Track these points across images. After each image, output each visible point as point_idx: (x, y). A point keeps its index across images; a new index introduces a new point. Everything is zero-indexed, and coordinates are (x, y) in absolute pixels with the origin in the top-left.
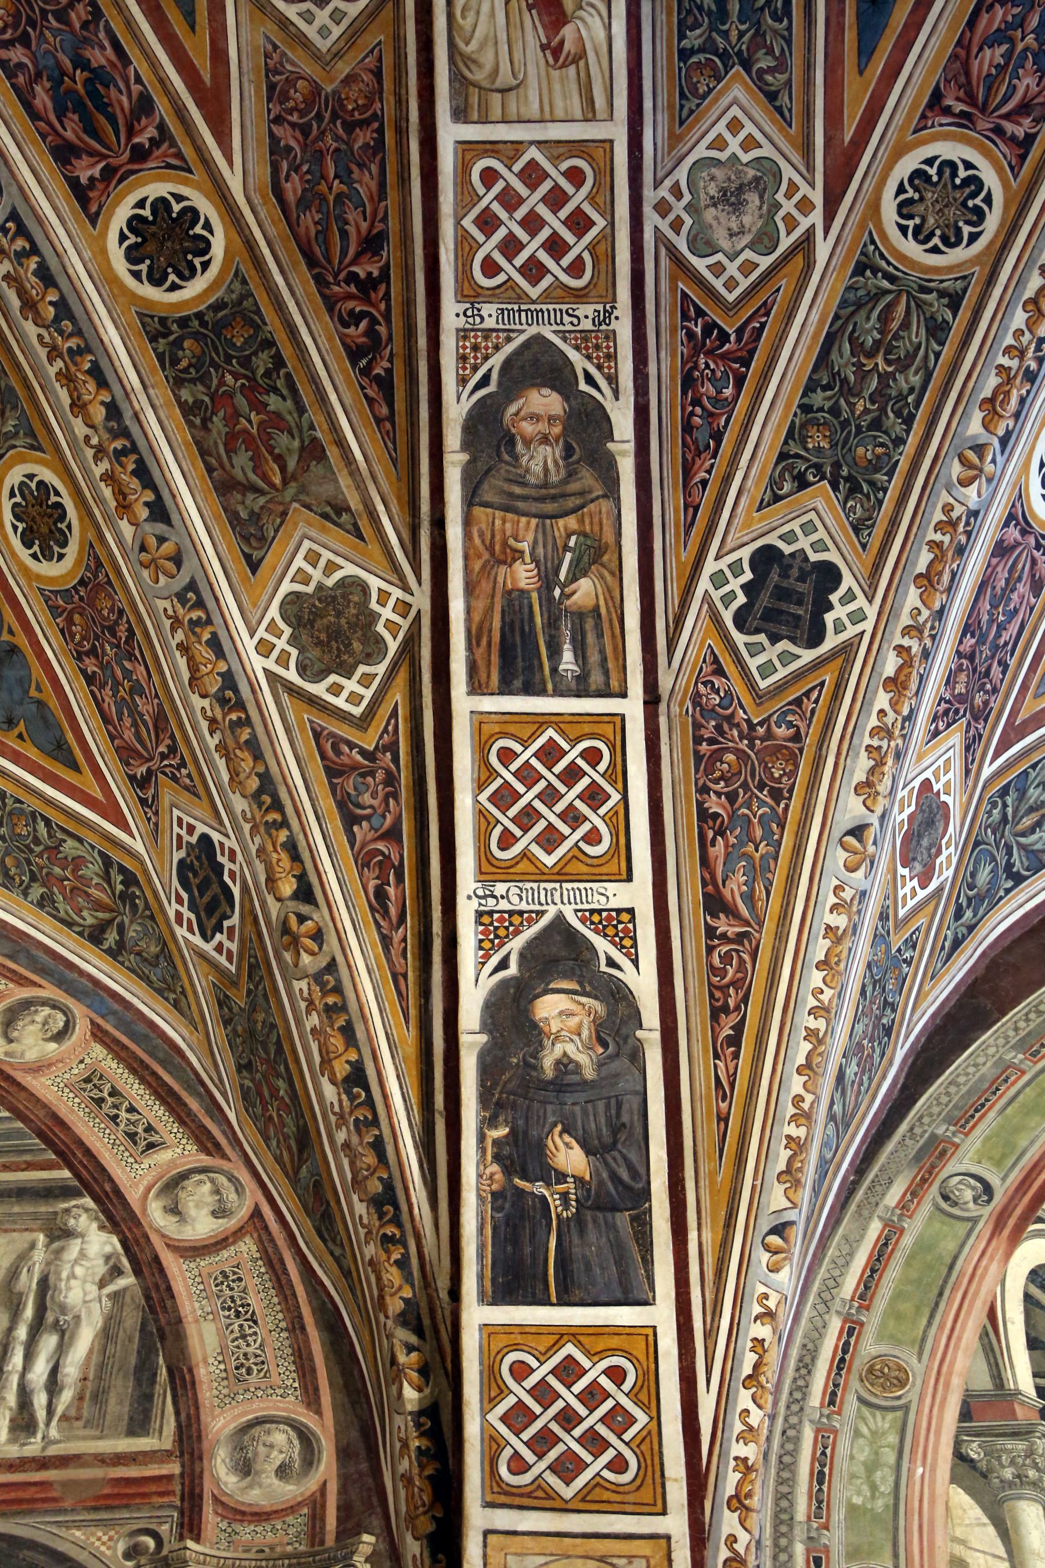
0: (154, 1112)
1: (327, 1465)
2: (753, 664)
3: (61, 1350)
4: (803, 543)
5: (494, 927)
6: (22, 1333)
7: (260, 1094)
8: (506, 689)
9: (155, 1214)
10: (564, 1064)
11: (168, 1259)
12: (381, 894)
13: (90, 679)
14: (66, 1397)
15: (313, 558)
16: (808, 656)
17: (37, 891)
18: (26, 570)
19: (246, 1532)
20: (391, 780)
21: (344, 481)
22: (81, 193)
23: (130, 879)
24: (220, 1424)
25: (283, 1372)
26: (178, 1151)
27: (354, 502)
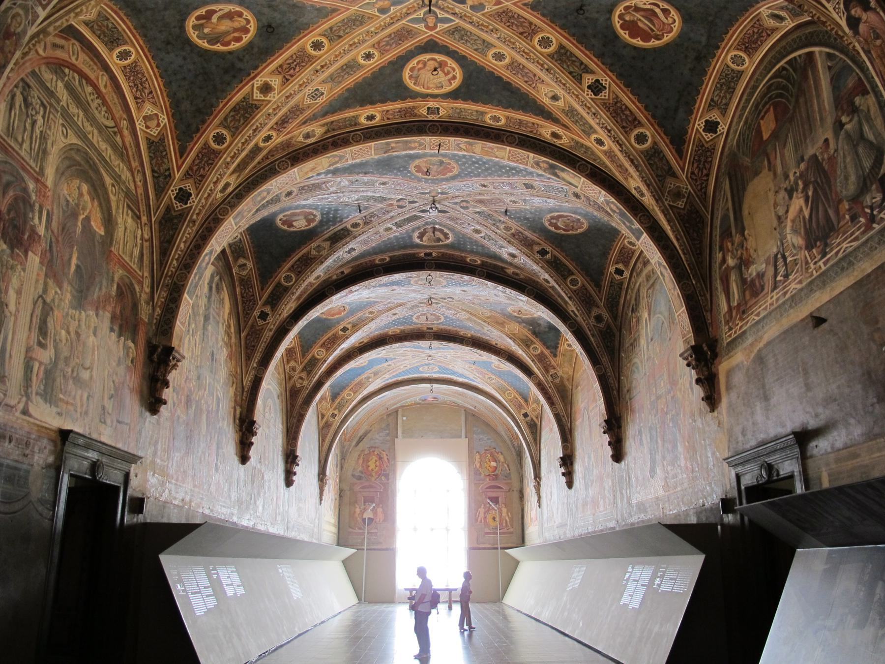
13: (197, 156)
22: (272, 127)
23: (170, 175)
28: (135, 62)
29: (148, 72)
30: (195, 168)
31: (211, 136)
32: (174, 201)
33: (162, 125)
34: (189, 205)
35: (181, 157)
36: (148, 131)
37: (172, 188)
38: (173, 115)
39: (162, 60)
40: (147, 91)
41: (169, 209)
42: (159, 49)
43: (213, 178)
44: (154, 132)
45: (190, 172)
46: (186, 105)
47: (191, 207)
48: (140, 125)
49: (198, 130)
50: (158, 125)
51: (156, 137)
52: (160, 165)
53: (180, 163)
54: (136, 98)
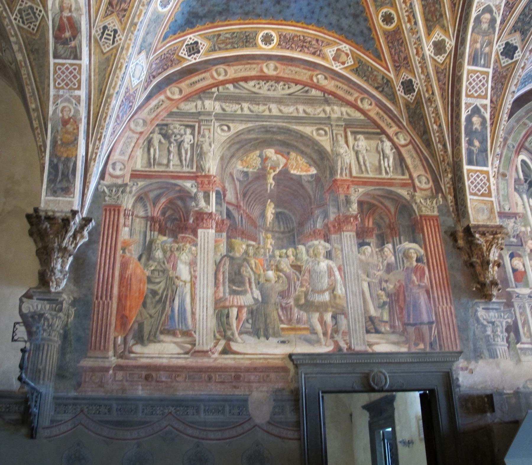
0: (390, 121)
1: (431, 183)
2: (502, 62)
3: (388, 161)
4: (514, 42)
5: (468, 105)
6: (382, 158)
7: (414, 122)
8: (473, 65)
9: (395, 139)
10: (476, 129)
11: (400, 147)
12: (442, 94)
13: (389, 47)
14: (391, 169)
15: (438, 35)
16: (510, 61)
17: (365, 78)
18: (381, 27)
19: (423, 192)
20: (445, 75)
21: (445, 22)
23: (388, 81)
24: (415, 175)
25: (421, 168)
26: (395, 128)
27: (446, 25)
28: (280, 36)
29: (298, 31)
30: (396, 58)
31: (382, 24)
32: (406, 97)
33: (349, 52)
34: (416, 90)
35: (381, 60)
36: (346, 65)
37: (397, 89)
38: (346, 38)
39: (293, 15)
40: (314, 42)
41: (407, 105)
42: (280, 12)
43: (412, 51)
44: (350, 62)
45: (397, 65)
46: (345, 23)
47: (419, 90)
48: (337, 67)
49: (370, 29)
50: (347, 55)
51: (354, 64)
52: (375, 80)
53: (385, 65)
54: (314, 54)
